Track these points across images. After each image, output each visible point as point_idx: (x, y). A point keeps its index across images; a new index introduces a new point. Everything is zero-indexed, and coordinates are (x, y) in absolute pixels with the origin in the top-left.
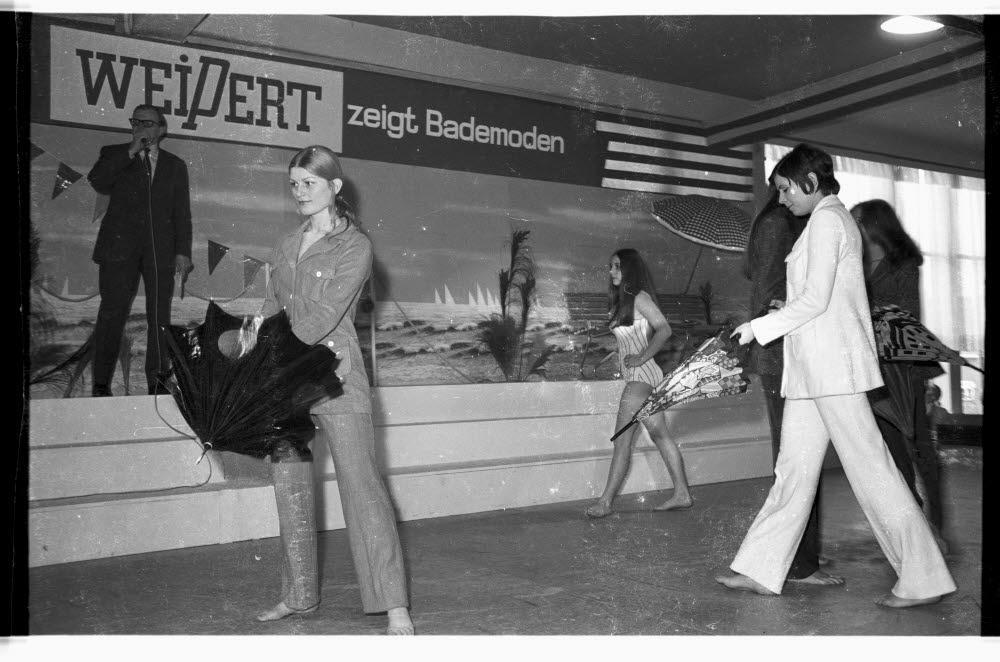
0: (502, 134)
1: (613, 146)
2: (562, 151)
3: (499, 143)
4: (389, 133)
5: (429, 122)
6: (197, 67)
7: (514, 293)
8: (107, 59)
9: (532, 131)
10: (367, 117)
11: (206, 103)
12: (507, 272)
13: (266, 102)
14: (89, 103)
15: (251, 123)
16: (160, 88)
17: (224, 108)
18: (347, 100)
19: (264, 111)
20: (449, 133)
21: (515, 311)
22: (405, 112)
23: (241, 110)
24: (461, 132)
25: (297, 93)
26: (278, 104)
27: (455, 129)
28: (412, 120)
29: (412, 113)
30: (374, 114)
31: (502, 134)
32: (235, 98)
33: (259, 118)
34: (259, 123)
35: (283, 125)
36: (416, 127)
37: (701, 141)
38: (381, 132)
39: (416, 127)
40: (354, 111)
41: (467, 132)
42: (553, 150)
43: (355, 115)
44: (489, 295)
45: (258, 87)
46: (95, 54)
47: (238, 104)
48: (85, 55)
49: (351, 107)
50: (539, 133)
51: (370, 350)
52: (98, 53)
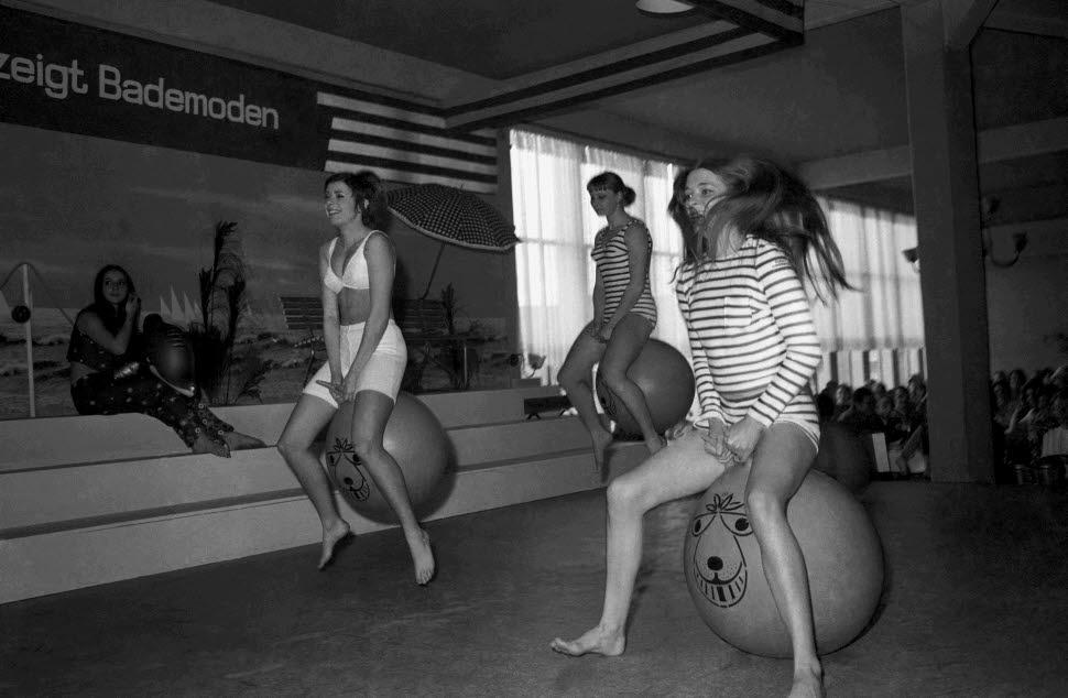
0: (200, 101)
1: (338, 124)
2: (276, 126)
3: (196, 112)
4: (48, 91)
5: (103, 81)
7: (219, 298)
9: (238, 99)
10: (15, 69)
12: (209, 272)
20: (130, 96)
21: (220, 319)
27: (139, 91)
28: (79, 76)
31: (200, 101)
36: (85, 87)
37: (439, 122)
39: (85, 87)
41: (154, 96)
42: (265, 125)
44: (186, 299)
51: (26, 371)
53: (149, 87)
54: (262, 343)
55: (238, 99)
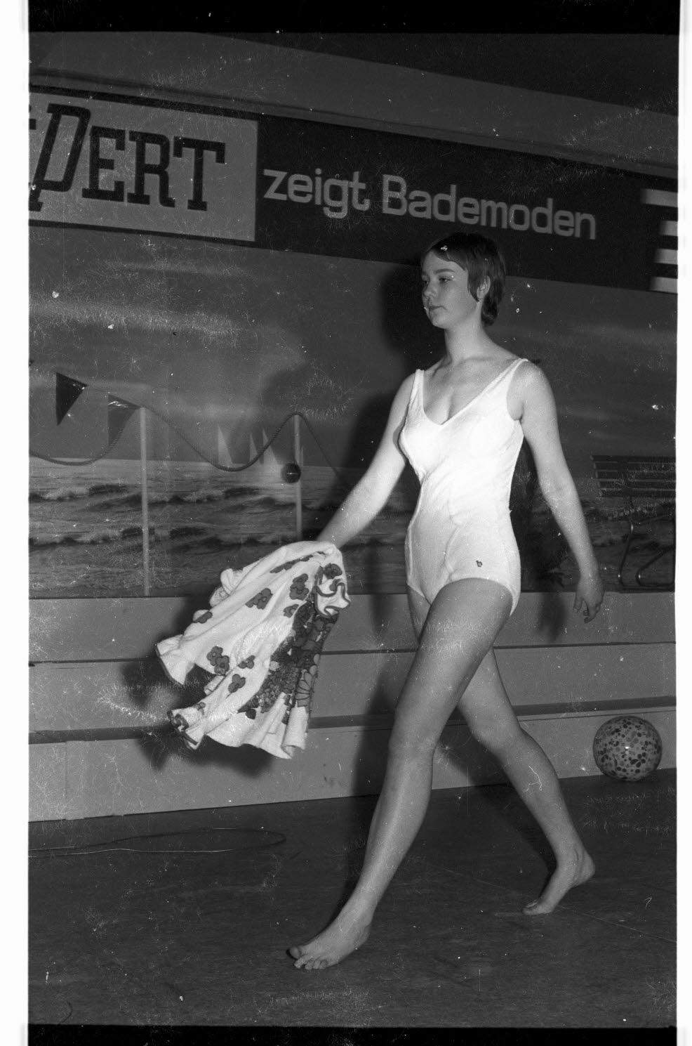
0: (499, 211)
2: (593, 236)
3: (494, 224)
5: (387, 194)
9: (545, 205)
10: (292, 188)
13: (143, 168)
16: (109, 165)
17: (82, 179)
18: (261, 166)
19: (140, 183)
22: (350, 179)
23: (106, 179)
24: (534, 222)
25: (189, 153)
26: (161, 170)
28: (361, 191)
29: (361, 180)
30: (304, 183)
31: (499, 211)
32: (98, 163)
35: (167, 201)
38: (313, 210)
40: (273, 179)
41: (444, 208)
42: (578, 235)
43: (275, 185)
45: (131, 145)
49: (268, 172)
50: (460, 195)
52: (131, 133)
53: (440, 196)
55: (545, 205)
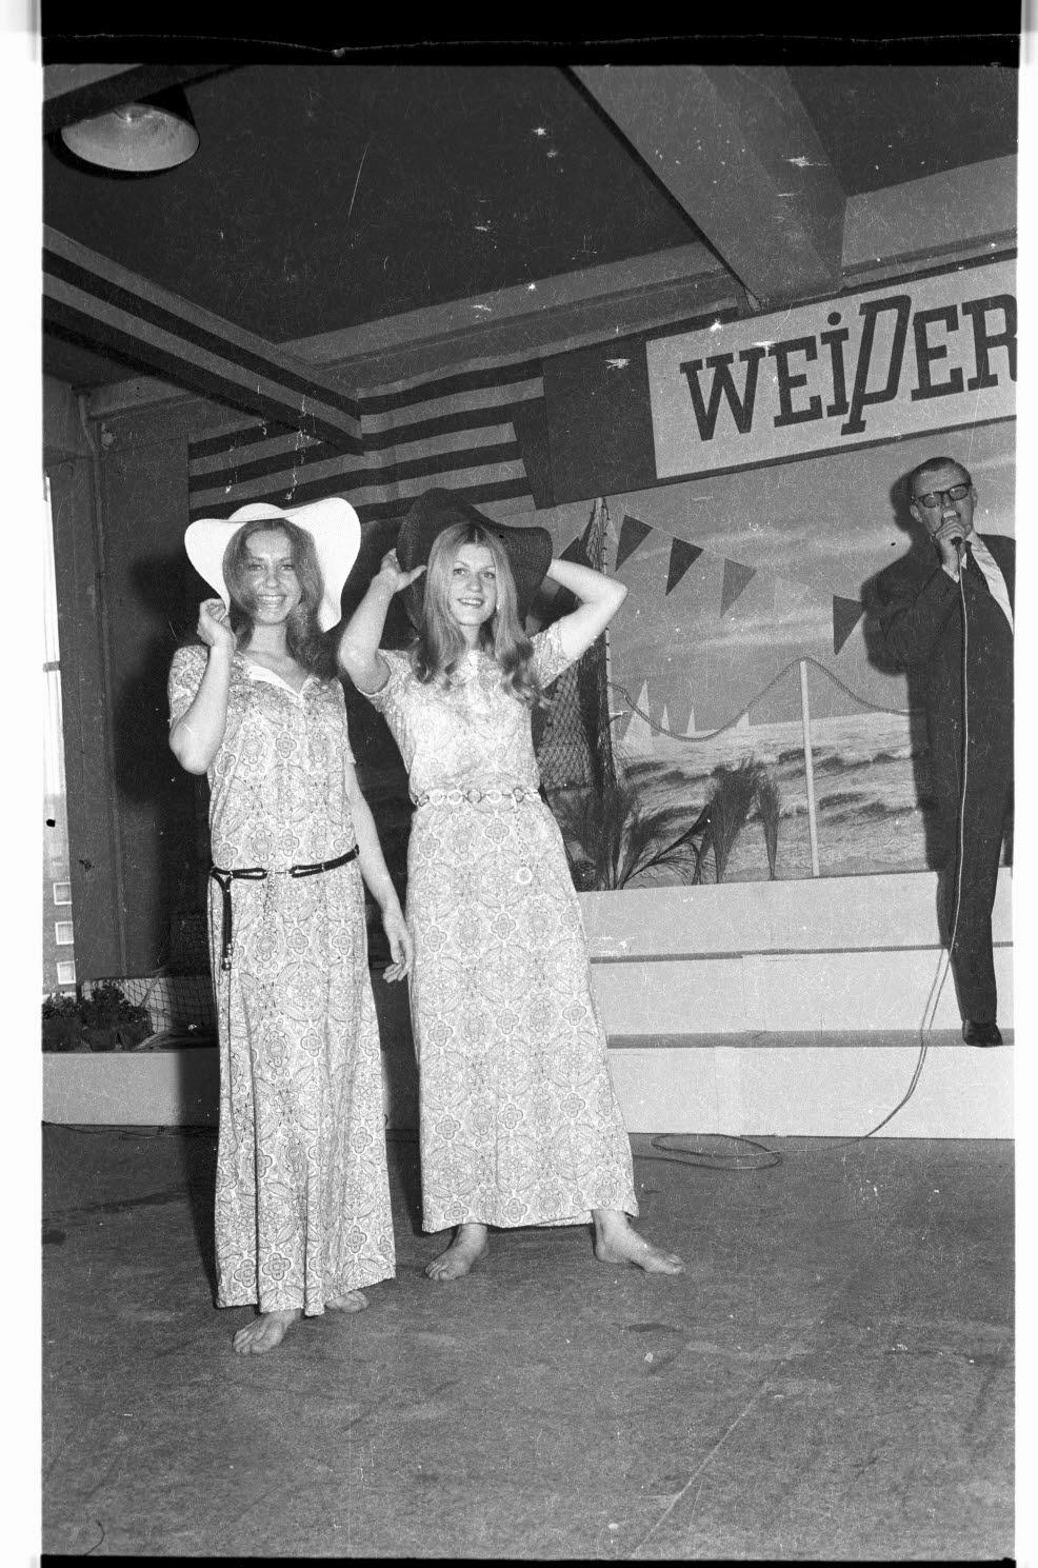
6: (854, 323)
8: (721, 362)
11: (877, 382)
13: (983, 343)
14: (741, 432)
15: (960, 389)
17: (909, 379)
23: (940, 373)
32: (926, 354)
33: (974, 375)
34: (973, 384)
45: (966, 322)
46: (704, 362)
47: (933, 364)
48: (691, 369)
54: (787, 768)
